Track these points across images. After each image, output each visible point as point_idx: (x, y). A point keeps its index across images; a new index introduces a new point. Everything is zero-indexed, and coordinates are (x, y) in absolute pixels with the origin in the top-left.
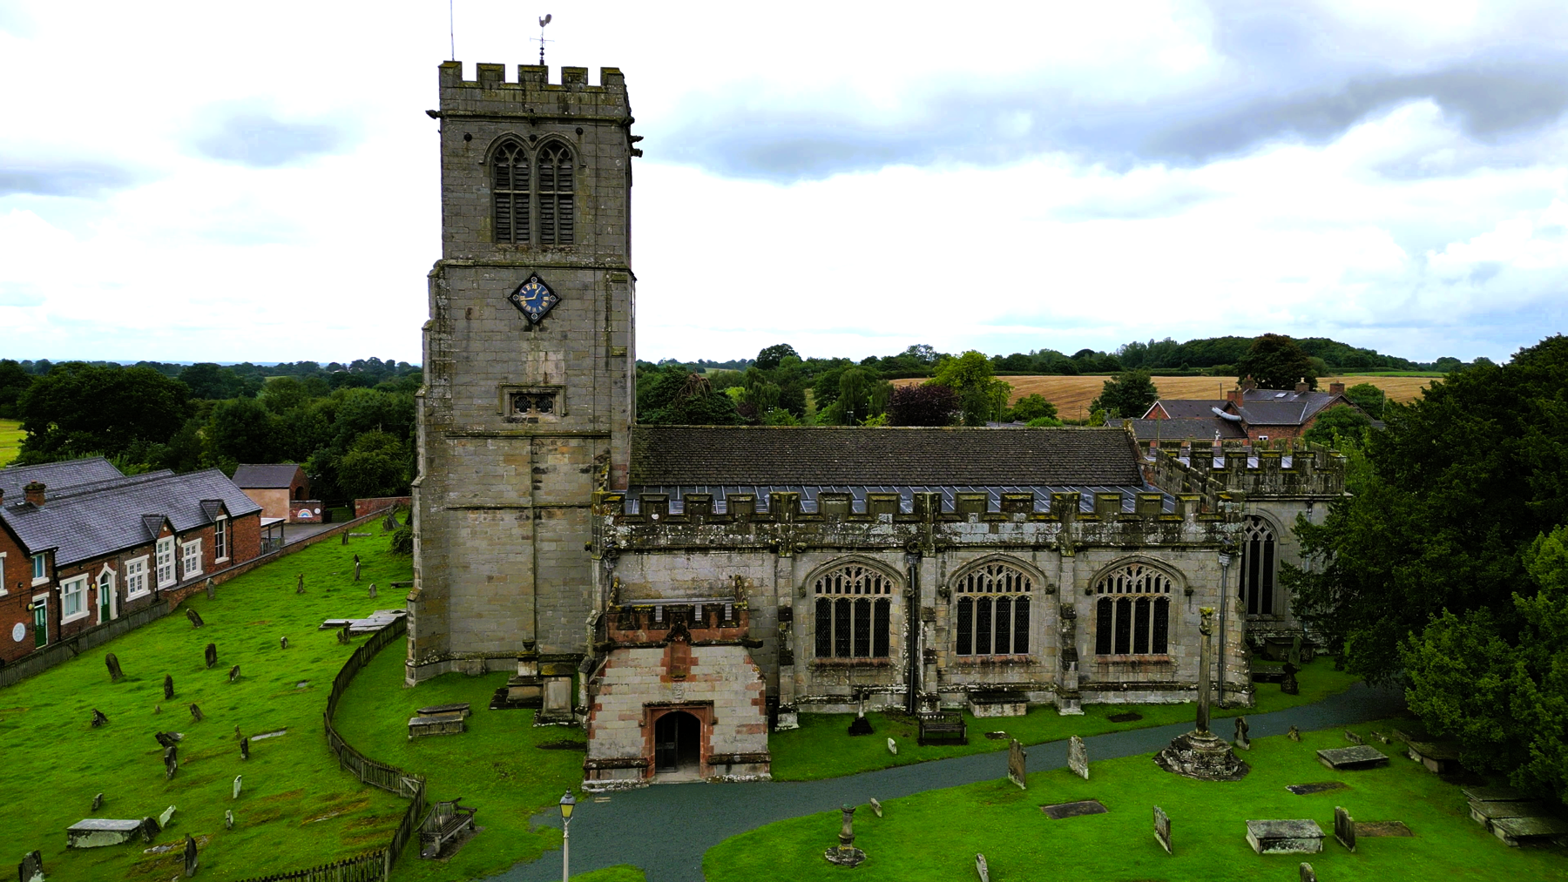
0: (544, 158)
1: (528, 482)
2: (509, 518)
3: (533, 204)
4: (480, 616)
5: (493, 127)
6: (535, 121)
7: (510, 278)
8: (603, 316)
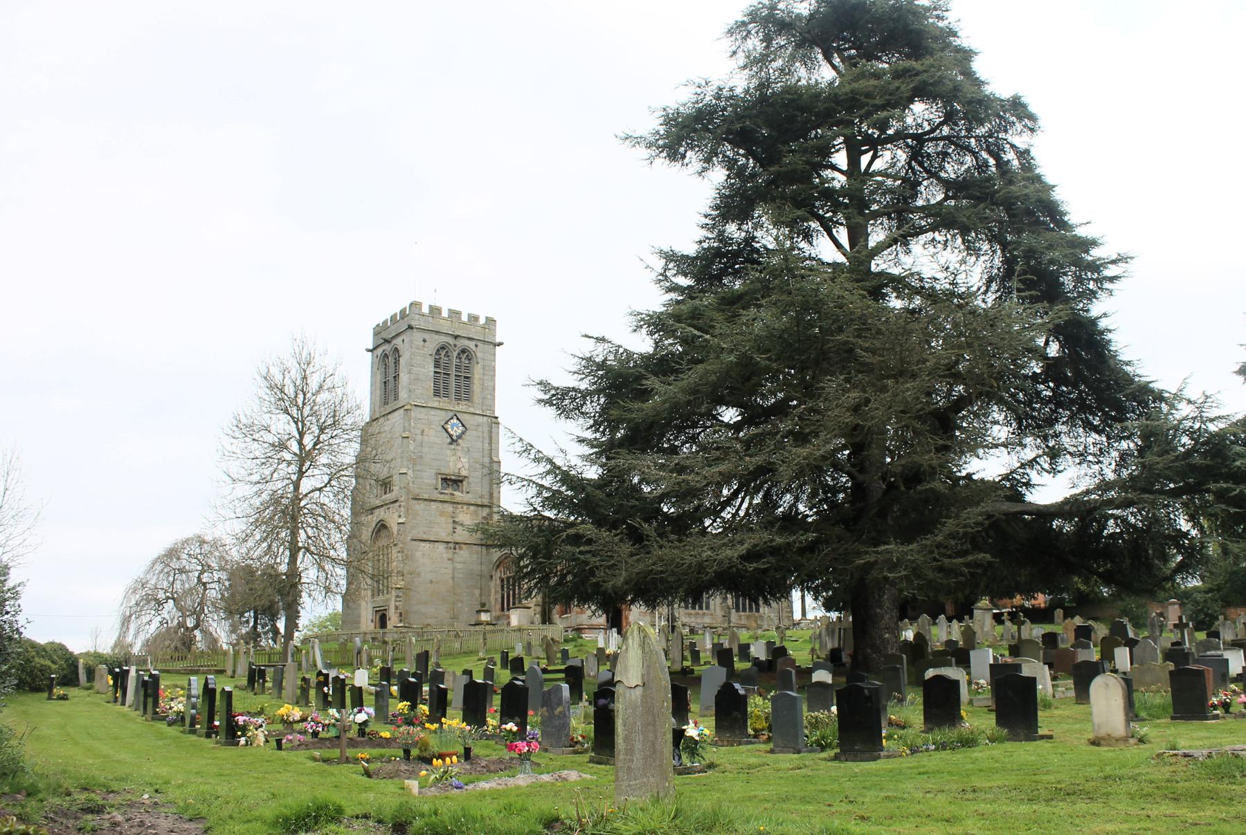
0: (459, 357)
1: (451, 526)
2: (441, 547)
3: (453, 377)
4: (425, 603)
5: (436, 337)
6: (456, 337)
7: (444, 416)
8: (487, 441)
